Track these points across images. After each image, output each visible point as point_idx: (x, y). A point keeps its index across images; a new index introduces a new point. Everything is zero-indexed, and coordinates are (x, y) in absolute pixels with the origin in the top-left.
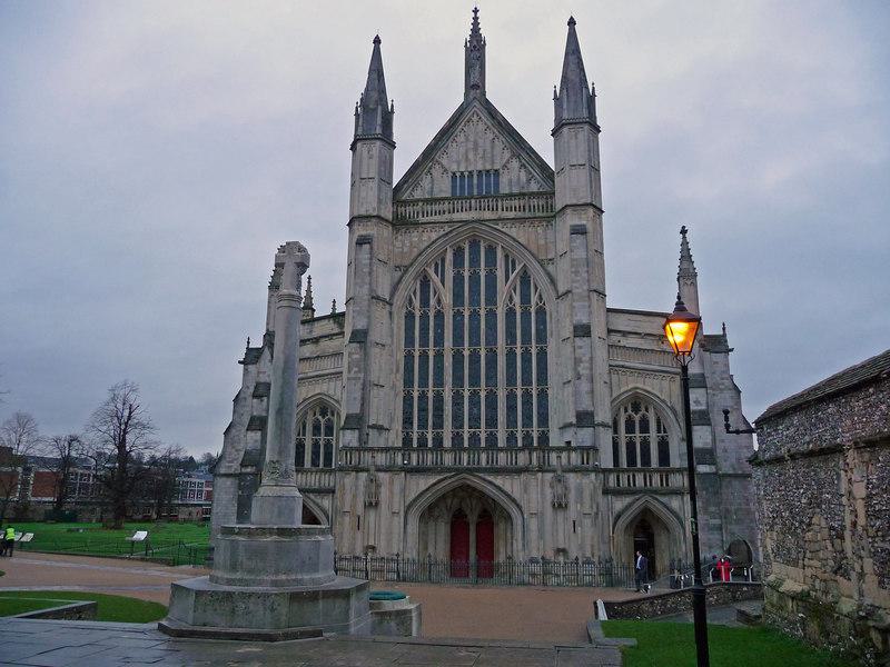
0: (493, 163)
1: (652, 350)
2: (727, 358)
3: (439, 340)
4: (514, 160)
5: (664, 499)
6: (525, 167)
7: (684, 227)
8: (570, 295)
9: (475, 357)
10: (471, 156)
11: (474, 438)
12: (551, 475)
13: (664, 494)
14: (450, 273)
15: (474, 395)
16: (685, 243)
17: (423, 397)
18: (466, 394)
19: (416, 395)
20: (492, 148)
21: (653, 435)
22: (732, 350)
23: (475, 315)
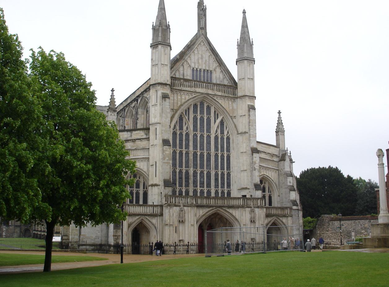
0: (209, 67)
1: (270, 160)
2: (292, 164)
3: (187, 146)
5: (281, 218)
6: (223, 72)
7: (279, 111)
8: (247, 134)
9: (202, 155)
10: (200, 61)
13: (281, 217)
14: (192, 116)
15: (202, 173)
16: (279, 118)
17: (181, 172)
18: (199, 172)
19: (178, 171)
21: (267, 194)
22: (294, 162)
23: (202, 136)
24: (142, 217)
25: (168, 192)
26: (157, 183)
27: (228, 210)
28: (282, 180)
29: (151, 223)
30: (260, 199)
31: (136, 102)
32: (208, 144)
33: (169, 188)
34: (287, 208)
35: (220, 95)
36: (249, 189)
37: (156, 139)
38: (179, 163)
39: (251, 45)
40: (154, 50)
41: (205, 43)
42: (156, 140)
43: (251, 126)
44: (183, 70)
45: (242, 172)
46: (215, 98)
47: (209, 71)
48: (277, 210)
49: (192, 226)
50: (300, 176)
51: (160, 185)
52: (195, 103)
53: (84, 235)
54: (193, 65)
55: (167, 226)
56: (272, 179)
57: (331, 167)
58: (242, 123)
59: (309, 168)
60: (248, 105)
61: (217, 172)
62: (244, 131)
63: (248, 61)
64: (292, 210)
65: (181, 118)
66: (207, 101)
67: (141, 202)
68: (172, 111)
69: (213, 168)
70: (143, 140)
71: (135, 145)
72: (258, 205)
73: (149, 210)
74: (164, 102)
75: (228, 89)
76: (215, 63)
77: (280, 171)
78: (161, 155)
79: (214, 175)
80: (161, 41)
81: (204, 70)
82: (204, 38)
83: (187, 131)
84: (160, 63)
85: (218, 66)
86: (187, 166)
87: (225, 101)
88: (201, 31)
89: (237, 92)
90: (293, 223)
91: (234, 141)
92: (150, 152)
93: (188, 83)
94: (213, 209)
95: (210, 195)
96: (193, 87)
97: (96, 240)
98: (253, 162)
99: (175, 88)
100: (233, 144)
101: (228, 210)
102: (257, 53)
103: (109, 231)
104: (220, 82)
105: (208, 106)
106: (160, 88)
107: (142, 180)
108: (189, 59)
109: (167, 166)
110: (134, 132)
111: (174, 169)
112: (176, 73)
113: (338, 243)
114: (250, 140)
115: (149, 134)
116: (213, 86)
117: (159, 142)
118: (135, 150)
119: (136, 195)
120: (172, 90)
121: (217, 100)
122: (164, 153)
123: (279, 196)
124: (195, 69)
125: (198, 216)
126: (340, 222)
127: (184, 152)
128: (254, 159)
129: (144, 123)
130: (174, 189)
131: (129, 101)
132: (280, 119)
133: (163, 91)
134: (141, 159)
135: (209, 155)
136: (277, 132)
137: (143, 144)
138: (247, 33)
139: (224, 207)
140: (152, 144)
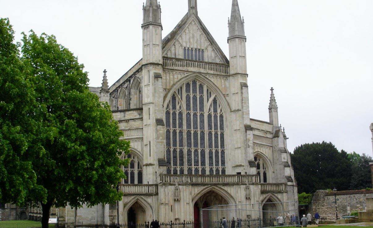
0: (201, 46)
1: (263, 137)
2: (286, 141)
3: (181, 125)
4: (210, 47)
5: (276, 195)
6: (214, 51)
7: (272, 88)
8: (240, 112)
9: (196, 134)
10: (191, 40)
11: (197, 170)
12: (245, 186)
13: (276, 193)
14: (184, 95)
15: (196, 151)
16: (272, 95)
17: (175, 151)
18: (193, 151)
19: (172, 150)
20: (201, 39)
21: (262, 171)
22: (288, 138)
23: (195, 115)
24: (138, 197)
25: (163, 171)
26: (152, 162)
27: (223, 187)
28: (276, 157)
29: (147, 202)
30: (255, 175)
31: (128, 83)
32: (201, 123)
33: (164, 167)
34: (281, 184)
35: (213, 73)
36: (243, 166)
37: (150, 119)
38: (173, 142)
39: (242, 23)
40: (146, 31)
41: (196, 23)
42: (149, 120)
43: (244, 104)
44: (175, 50)
45: (236, 149)
46: (207, 77)
47: (201, 50)
48: (272, 186)
49: (188, 204)
50: (295, 152)
51: (154, 165)
52: (187, 82)
54: (184, 45)
55: (163, 205)
56: (267, 156)
57: (325, 142)
58: (235, 100)
59: (303, 143)
60: (241, 83)
61: (211, 150)
62: (237, 108)
63: (240, 39)
64: (287, 186)
65: (174, 98)
66: (199, 80)
67: (136, 182)
68: (165, 90)
69: (207, 146)
70: (136, 120)
71: (129, 125)
72: (253, 181)
73: (144, 190)
74: (156, 81)
75: (220, 67)
76: (206, 41)
77: (274, 147)
78: (155, 134)
79: (208, 153)
80: (151, 21)
81: (196, 49)
82: (195, 17)
83: (181, 110)
84: (151, 43)
85: (209, 44)
86: (181, 145)
87: (218, 79)
88: (191, 11)
89: (229, 70)
90: (288, 199)
91: (228, 119)
92: (144, 132)
93: (180, 62)
94: (208, 187)
95: (205, 173)
96: (185, 66)
97: (92, 221)
98: (246, 139)
99: (167, 67)
100: (227, 122)
101: (223, 187)
102: (248, 31)
103: (105, 211)
104: (212, 60)
105: (201, 84)
106: (152, 68)
107: (137, 160)
108: (180, 38)
109: (161, 145)
110: (127, 113)
111: (168, 148)
112: (167, 52)
113: (334, 217)
114: (243, 118)
115: (142, 114)
116: (205, 65)
117: (152, 121)
118: (129, 130)
119: (131, 175)
120: (164, 69)
121: (209, 78)
122: (158, 133)
123: (274, 172)
124: (187, 48)
125: (193, 194)
126: (335, 197)
127: (178, 131)
128: (248, 136)
129: (137, 103)
130: (169, 168)
131: (121, 82)
132: (272, 95)
133: (155, 71)
134: (135, 139)
135: (203, 133)
136: (270, 109)
137: (137, 124)
138: (237, 11)
139: (219, 185)
140: (145, 124)
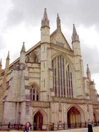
15: (62, 88)
26: (46, 90)
39: (78, 36)
53: (5, 119)
62: (78, 70)
110: (33, 64)
117: (46, 69)
137: (38, 70)
